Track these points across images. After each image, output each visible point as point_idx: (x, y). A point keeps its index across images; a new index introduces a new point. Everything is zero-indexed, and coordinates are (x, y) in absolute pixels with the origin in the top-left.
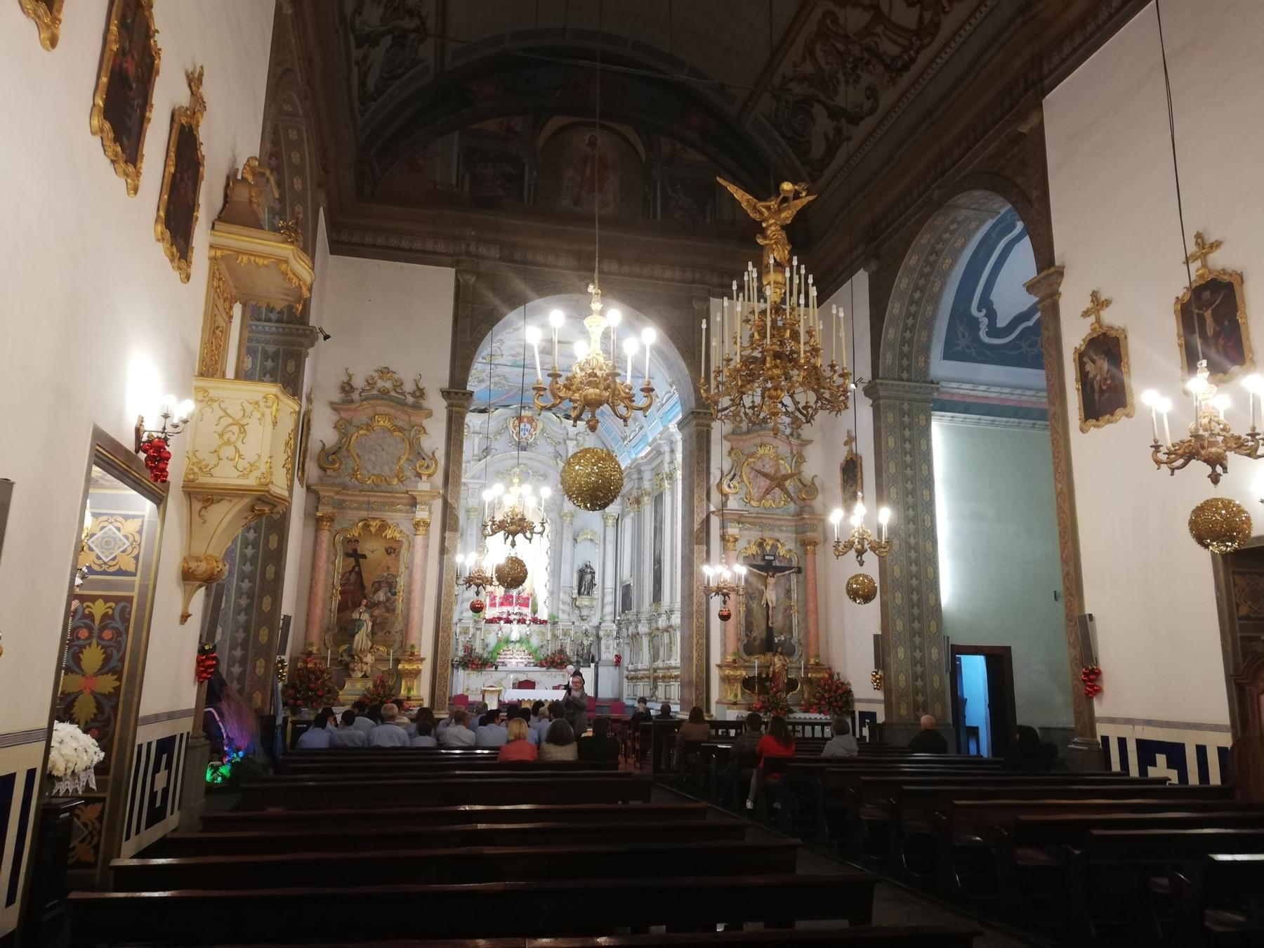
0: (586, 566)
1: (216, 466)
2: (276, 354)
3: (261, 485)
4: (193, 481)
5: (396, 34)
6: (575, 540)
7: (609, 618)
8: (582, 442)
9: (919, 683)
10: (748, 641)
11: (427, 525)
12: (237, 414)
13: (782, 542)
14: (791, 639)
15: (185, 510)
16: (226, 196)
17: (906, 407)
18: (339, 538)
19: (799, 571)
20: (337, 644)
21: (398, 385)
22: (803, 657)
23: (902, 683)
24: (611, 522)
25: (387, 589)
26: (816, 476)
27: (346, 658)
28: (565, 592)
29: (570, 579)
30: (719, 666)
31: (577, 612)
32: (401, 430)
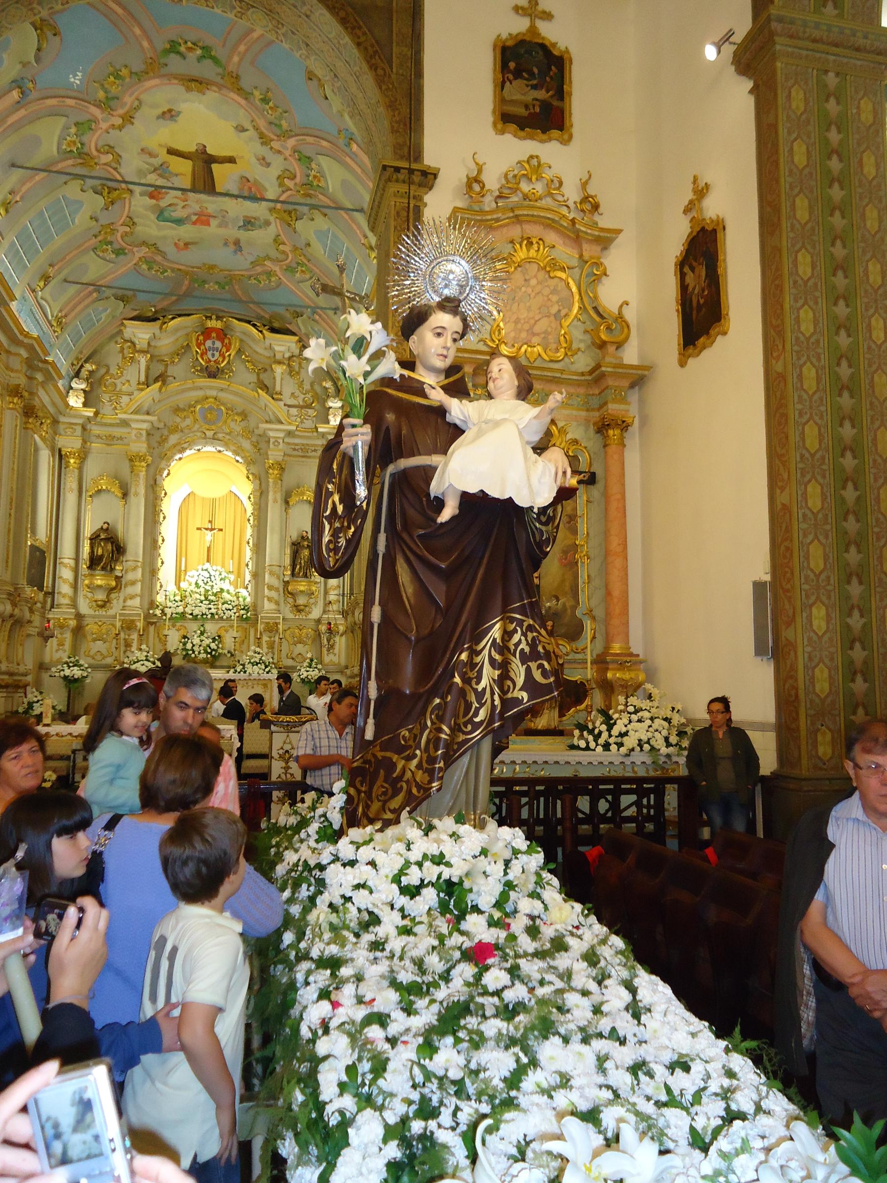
0: (303, 537)
6: (287, 502)
8: (297, 369)
13: (560, 424)
14: (575, 607)
17: (831, 79)
23: (822, 686)
28: (271, 573)
31: (291, 600)
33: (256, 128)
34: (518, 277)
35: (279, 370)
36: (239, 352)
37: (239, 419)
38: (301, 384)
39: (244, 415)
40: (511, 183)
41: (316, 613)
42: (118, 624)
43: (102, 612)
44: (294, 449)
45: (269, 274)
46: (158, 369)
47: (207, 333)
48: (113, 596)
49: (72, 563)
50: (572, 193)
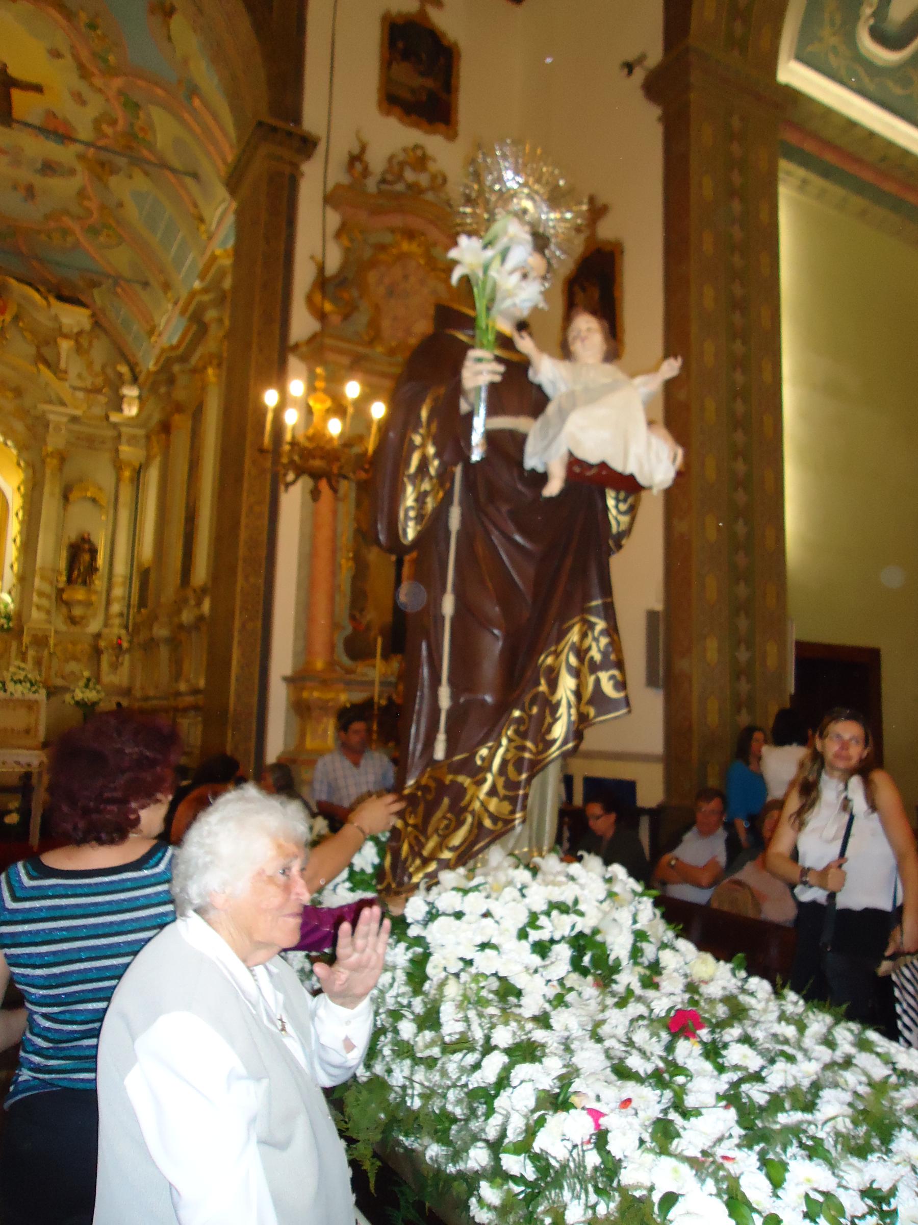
7: (117, 621)
17: (736, 122)
23: (713, 719)
24: (127, 474)
31: (64, 610)
33: (76, 57)
35: (65, 346)
36: (17, 318)
37: (10, 395)
38: (90, 365)
39: (18, 392)
44: (78, 438)
45: (66, 232)
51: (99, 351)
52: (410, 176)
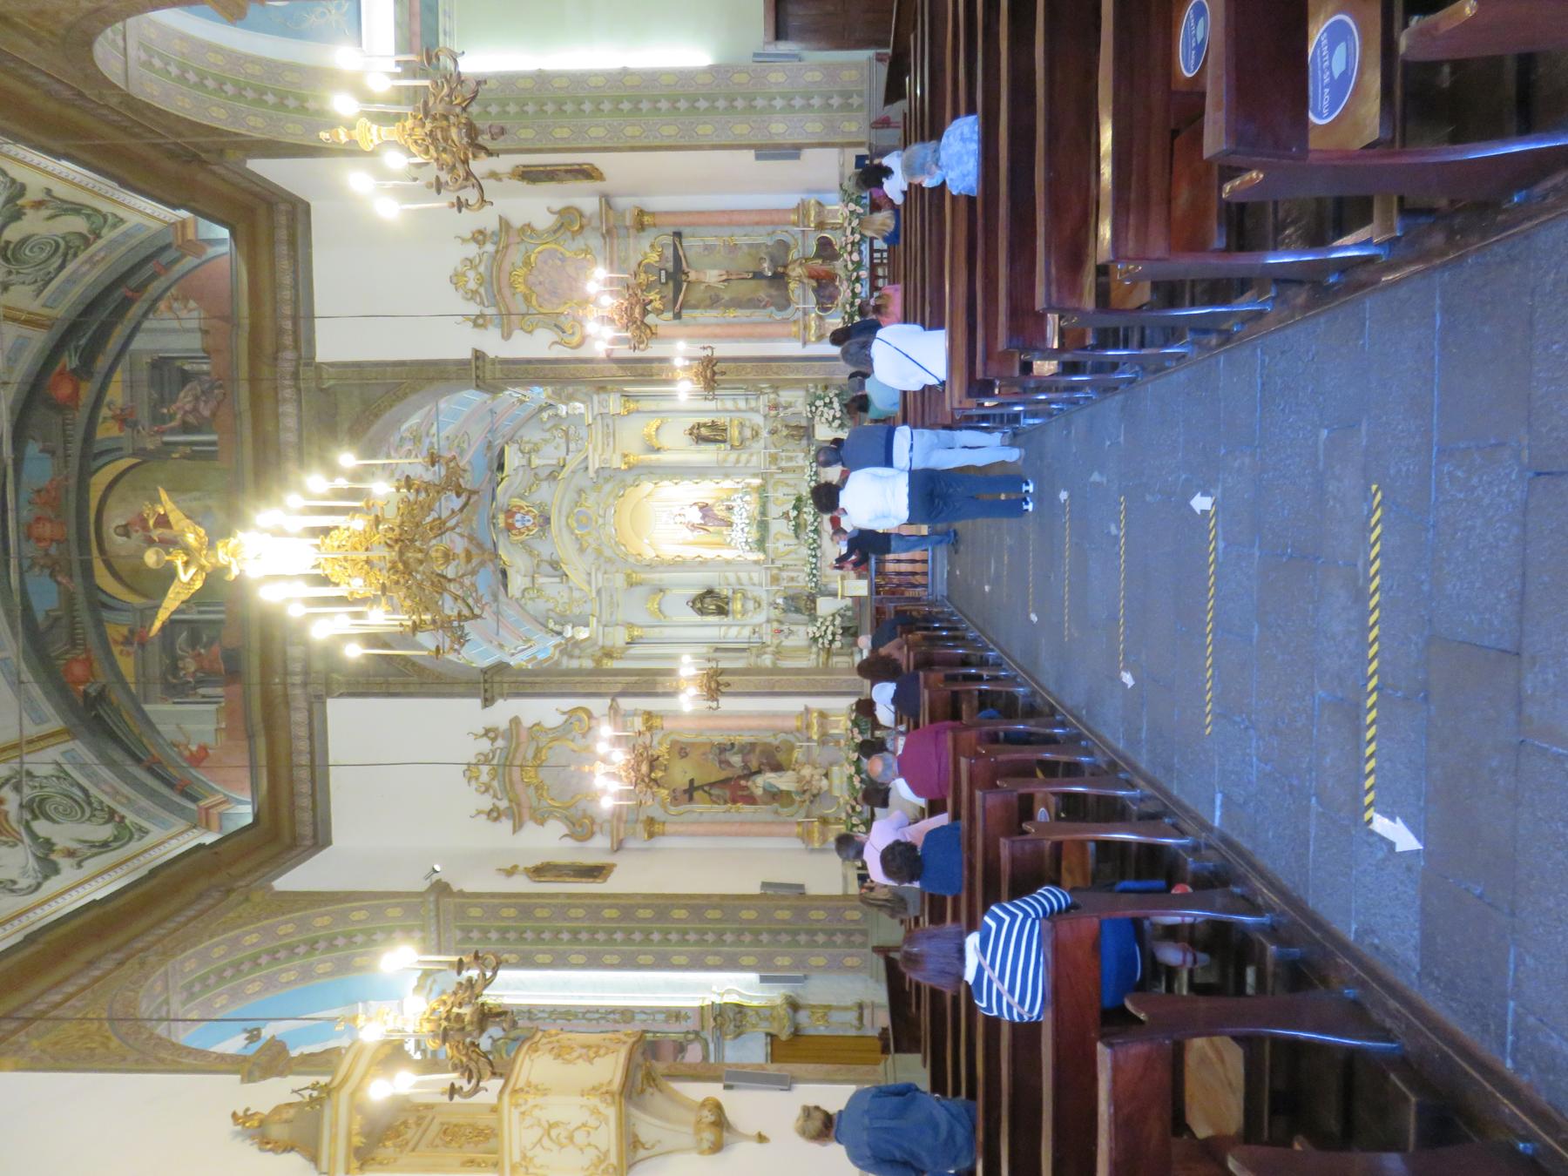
1: (597, 1148)
2: (462, 929)
3: (614, 1102)
4: (615, 1168)
5: (29, 817)
8: (531, 446)
9: (816, 101)
10: (772, 305)
11: (649, 715)
12: (536, 1133)
13: (640, 258)
14: (767, 246)
15: (648, 1163)
16: (289, 1148)
18: (673, 810)
19: (678, 235)
20: (792, 802)
21: (486, 759)
22: (787, 228)
24: (632, 406)
25: (727, 754)
26: (548, 209)
27: (807, 796)
29: (707, 454)
30: (805, 343)
31: (748, 443)
32: (538, 751)
34: (538, 289)
35: (536, 462)
36: (521, 497)
39: (580, 491)
40: (472, 295)
41: (758, 420)
42: (775, 588)
43: (764, 604)
46: (546, 568)
47: (510, 528)
48: (750, 595)
49: (723, 629)
50: (472, 250)
51: (532, 435)
52: (472, 285)
